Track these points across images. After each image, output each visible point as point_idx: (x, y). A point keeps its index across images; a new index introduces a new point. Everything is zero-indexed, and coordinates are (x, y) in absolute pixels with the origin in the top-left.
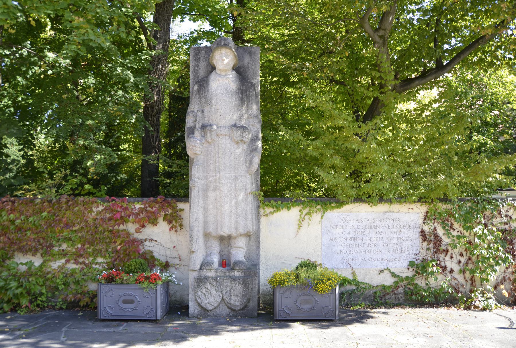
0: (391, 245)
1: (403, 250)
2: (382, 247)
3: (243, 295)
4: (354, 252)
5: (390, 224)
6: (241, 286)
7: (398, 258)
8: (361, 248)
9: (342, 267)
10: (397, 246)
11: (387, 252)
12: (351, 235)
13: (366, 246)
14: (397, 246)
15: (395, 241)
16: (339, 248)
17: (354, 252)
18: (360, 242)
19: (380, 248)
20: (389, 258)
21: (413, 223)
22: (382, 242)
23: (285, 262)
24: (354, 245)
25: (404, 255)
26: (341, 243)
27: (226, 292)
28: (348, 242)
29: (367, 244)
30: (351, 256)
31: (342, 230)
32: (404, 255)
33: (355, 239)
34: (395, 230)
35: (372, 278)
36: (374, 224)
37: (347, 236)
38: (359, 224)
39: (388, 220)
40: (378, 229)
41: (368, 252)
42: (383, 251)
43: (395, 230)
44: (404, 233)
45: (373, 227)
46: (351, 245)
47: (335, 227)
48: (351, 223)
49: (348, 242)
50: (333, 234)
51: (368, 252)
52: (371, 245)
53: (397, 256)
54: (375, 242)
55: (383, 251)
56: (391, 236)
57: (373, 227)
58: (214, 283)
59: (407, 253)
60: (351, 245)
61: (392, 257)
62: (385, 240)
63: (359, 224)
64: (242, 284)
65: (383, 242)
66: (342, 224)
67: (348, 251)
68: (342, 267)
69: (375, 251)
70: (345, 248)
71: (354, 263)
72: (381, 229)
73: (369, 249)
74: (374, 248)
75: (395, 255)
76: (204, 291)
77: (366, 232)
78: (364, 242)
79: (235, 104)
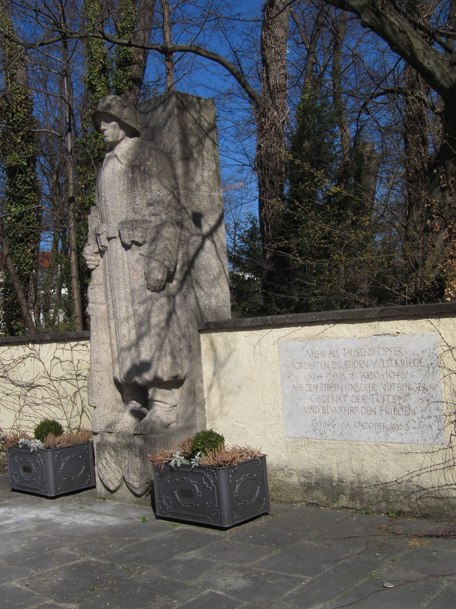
0: (391, 399)
1: (412, 408)
2: (376, 403)
3: (141, 473)
4: (330, 411)
5: (386, 358)
6: (138, 459)
7: (404, 423)
8: (340, 404)
9: (314, 436)
10: (402, 402)
11: (384, 413)
12: (324, 380)
13: (348, 400)
14: (402, 402)
15: (395, 392)
16: (308, 403)
17: (330, 411)
18: (338, 393)
19: (371, 405)
20: (388, 424)
21: (425, 355)
22: (373, 392)
23: (237, 424)
24: (330, 397)
25: (415, 418)
26: (310, 394)
27: (125, 467)
28: (320, 393)
29: (350, 395)
30: (326, 418)
31: (310, 371)
32: (415, 418)
33: (330, 387)
34: (395, 370)
35: (363, 461)
36: (358, 359)
37: (318, 382)
38: (335, 359)
39: (381, 352)
40: (366, 369)
41: (352, 410)
42: (378, 410)
43: (395, 370)
44: (412, 376)
45: (356, 364)
46: (324, 398)
47: (298, 366)
48: (321, 359)
49: (320, 393)
50: (296, 378)
51: (352, 410)
52: (357, 399)
53: (402, 419)
54: (362, 393)
55: (378, 410)
56: (390, 381)
57: (356, 364)
58: (112, 453)
59: (420, 415)
60: (324, 398)
61: (394, 422)
62: (380, 389)
63: (335, 359)
64: (140, 457)
65: (376, 394)
66: (308, 360)
67: (321, 409)
68: (314, 436)
69: (364, 410)
70: (317, 404)
71: (332, 430)
72: (371, 369)
73: (353, 405)
74: (362, 404)
75: (399, 418)
76: (104, 461)
77: (347, 376)
78: (345, 392)
79: (124, 190)
